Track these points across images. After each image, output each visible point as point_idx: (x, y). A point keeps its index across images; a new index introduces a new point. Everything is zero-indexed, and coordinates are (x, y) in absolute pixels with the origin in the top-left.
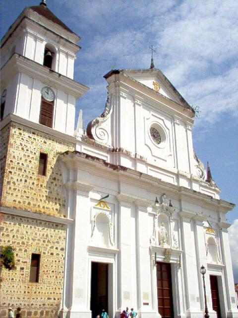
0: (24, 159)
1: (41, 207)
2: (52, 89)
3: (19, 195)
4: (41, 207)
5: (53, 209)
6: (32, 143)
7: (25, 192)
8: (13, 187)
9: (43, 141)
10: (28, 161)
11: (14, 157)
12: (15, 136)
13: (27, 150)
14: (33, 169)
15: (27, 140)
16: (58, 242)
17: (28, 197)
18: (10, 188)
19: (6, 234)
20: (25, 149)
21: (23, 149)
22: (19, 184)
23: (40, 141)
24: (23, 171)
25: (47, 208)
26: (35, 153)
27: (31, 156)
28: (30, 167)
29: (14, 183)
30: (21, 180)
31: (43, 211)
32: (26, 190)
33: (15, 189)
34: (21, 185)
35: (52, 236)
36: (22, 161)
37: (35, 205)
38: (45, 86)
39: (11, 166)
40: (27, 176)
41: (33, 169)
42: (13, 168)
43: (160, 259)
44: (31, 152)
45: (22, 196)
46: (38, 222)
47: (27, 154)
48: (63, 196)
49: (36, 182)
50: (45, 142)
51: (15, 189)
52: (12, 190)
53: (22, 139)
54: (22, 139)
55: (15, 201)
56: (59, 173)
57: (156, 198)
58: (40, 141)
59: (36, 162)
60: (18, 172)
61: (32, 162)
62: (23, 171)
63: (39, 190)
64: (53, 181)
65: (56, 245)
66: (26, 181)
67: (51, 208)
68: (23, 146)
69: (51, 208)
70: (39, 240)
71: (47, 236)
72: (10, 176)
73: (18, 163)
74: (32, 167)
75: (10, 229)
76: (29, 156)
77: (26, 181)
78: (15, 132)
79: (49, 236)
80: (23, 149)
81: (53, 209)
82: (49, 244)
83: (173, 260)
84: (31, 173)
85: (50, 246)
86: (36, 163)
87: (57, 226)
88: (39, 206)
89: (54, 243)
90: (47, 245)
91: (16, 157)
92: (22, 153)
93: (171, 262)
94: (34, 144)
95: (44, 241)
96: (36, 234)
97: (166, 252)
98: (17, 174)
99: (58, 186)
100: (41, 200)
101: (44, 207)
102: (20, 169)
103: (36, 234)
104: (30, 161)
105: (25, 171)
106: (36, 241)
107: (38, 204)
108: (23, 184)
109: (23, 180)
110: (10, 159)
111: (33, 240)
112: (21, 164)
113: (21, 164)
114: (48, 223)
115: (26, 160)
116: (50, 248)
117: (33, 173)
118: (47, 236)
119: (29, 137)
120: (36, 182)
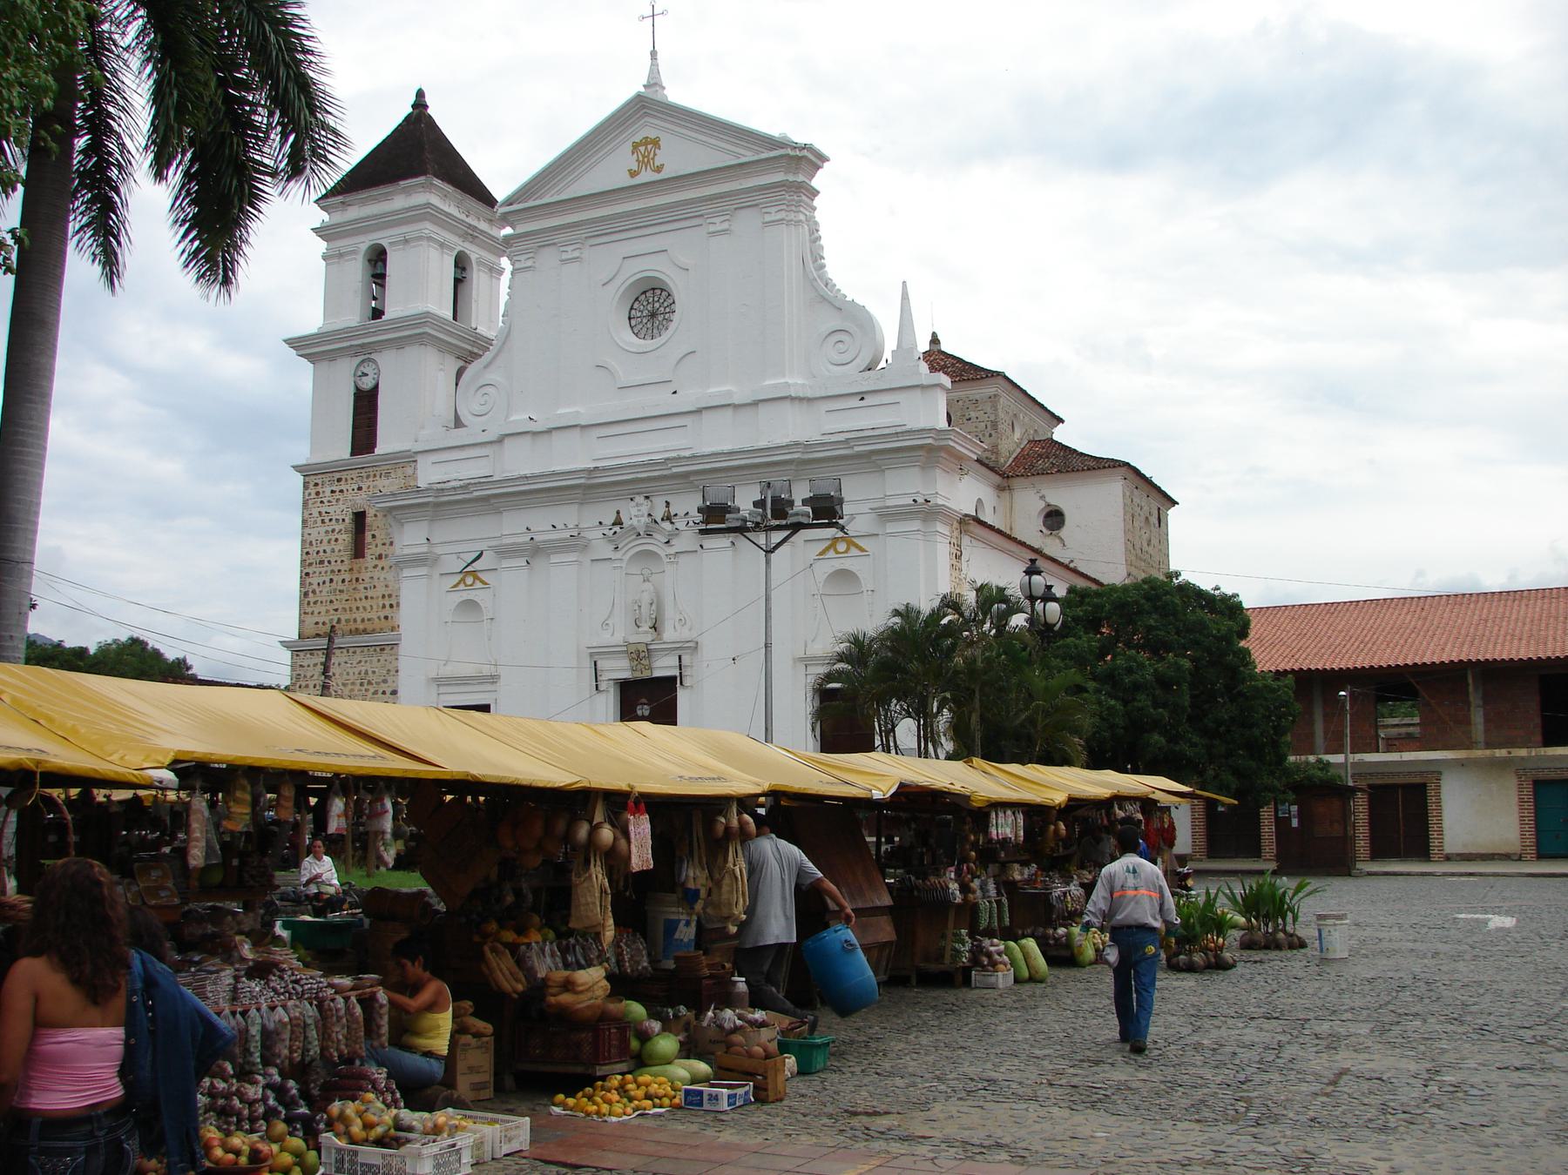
0: (325, 541)
1: (359, 620)
2: (372, 356)
3: (323, 609)
4: (359, 620)
5: (379, 618)
6: (338, 500)
7: (331, 602)
8: (312, 600)
9: (356, 487)
10: (333, 542)
11: (311, 544)
12: (310, 502)
13: (331, 520)
14: (342, 553)
15: (329, 502)
16: (385, 681)
17: (336, 610)
18: (309, 603)
19: (304, 684)
20: (327, 520)
21: (323, 521)
22: (321, 592)
23: (350, 491)
24: (326, 563)
25: (369, 620)
26: (343, 520)
27: (337, 528)
28: (336, 550)
29: (314, 592)
30: (324, 583)
31: (361, 627)
32: (333, 598)
33: (315, 603)
34: (323, 594)
35: (374, 672)
36: (325, 546)
37: (347, 621)
38: (360, 359)
39: (308, 562)
40: (332, 571)
41: (342, 553)
42: (310, 564)
43: (621, 669)
44: (337, 520)
45: (327, 611)
46: (351, 650)
47: (330, 529)
48: (397, 586)
49: (347, 577)
50: (360, 489)
51: (315, 603)
52: (312, 604)
53: (322, 502)
54: (322, 502)
55: (317, 623)
56: (388, 542)
57: (618, 512)
58: (350, 491)
59: (344, 536)
60: (318, 570)
61: (340, 541)
62: (326, 563)
63: (354, 589)
64: (377, 562)
65: (384, 687)
66: (331, 580)
67: (375, 617)
68: (324, 514)
69: (375, 617)
70: (353, 684)
71: (366, 673)
72: (308, 580)
73: (318, 552)
74: (340, 551)
75: (309, 675)
76: (333, 531)
77: (331, 580)
78: (310, 494)
79: (370, 672)
80: (323, 521)
81: (379, 618)
82: (369, 687)
83: (663, 667)
84: (339, 562)
85: (372, 690)
86: (346, 539)
87: (382, 650)
88: (355, 620)
89: (378, 683)
90: (366, 690)
91: (314, 543)
92: (323, 530)
93: (657, 674)
94: (341, 502)
95: (362, 684)
96: (348, 674)
97: (640, 655)
98: (317, 574)
99: (387, 568)
100: (358, 608)
101: (363, 620)
102: (322, 562)
103: (348, 674)
104: (336, 540)
105: (329, 562)
106: (350, 687)
107: (354, 616)
108: (328, 589)
109: (328, 580)
110: (305, 551)
111: (344, 685)
112: (321, 553)
113: (321, 553)
114: (366, 649)
115: (329, 542)
116: (373, 694)
117: (342, 561)
118: (366, 673)
119: (333, 492)
120: (347, 577)
